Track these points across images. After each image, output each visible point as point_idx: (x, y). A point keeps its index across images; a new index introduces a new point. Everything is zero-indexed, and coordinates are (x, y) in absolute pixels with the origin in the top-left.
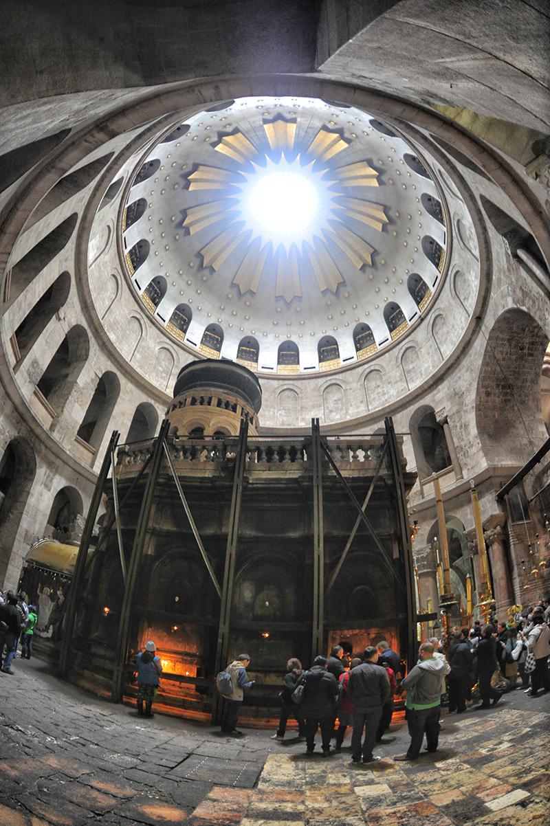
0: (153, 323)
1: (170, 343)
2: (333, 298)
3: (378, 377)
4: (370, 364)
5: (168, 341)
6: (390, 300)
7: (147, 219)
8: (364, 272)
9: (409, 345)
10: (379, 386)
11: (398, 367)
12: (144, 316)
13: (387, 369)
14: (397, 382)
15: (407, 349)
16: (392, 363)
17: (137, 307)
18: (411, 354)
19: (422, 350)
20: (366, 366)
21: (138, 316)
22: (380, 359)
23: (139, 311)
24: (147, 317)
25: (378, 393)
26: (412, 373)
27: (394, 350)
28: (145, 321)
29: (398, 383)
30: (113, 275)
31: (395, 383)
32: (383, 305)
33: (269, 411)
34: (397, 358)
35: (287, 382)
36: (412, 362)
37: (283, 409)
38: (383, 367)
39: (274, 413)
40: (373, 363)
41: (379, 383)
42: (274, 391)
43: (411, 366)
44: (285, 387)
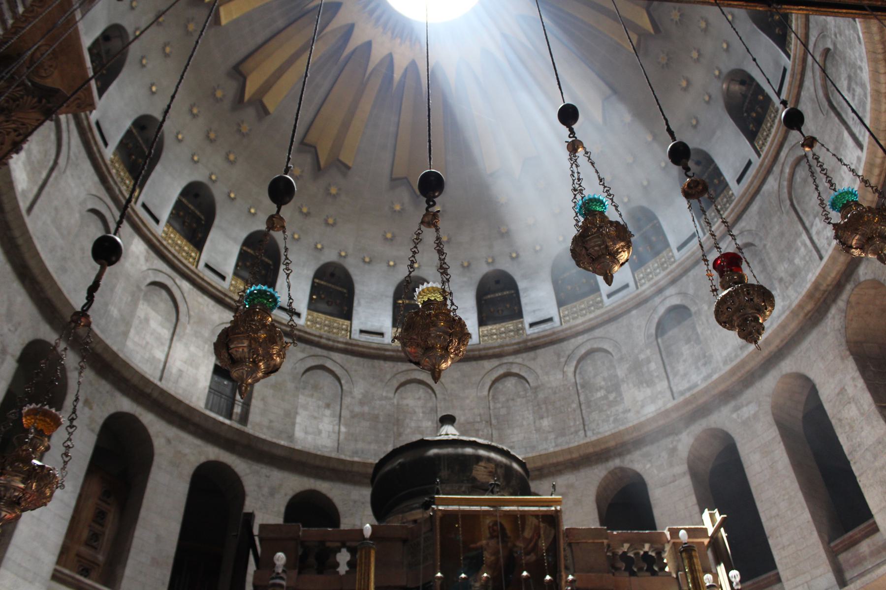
0: (535, 348)
1: (586, 337)
5: (580, 339)
7: (367, 267)
12: (510, 359)
17: (487, 364)
21: (501, 371)
23: (495, 362)
24: (516, 352)
28: (517, 363)
30: (403, 385)
33: (797, 250)
35: (783, 154)
37: (815, 217)
39: (805, 245)
42: (780, 201)
44: (787, 170)
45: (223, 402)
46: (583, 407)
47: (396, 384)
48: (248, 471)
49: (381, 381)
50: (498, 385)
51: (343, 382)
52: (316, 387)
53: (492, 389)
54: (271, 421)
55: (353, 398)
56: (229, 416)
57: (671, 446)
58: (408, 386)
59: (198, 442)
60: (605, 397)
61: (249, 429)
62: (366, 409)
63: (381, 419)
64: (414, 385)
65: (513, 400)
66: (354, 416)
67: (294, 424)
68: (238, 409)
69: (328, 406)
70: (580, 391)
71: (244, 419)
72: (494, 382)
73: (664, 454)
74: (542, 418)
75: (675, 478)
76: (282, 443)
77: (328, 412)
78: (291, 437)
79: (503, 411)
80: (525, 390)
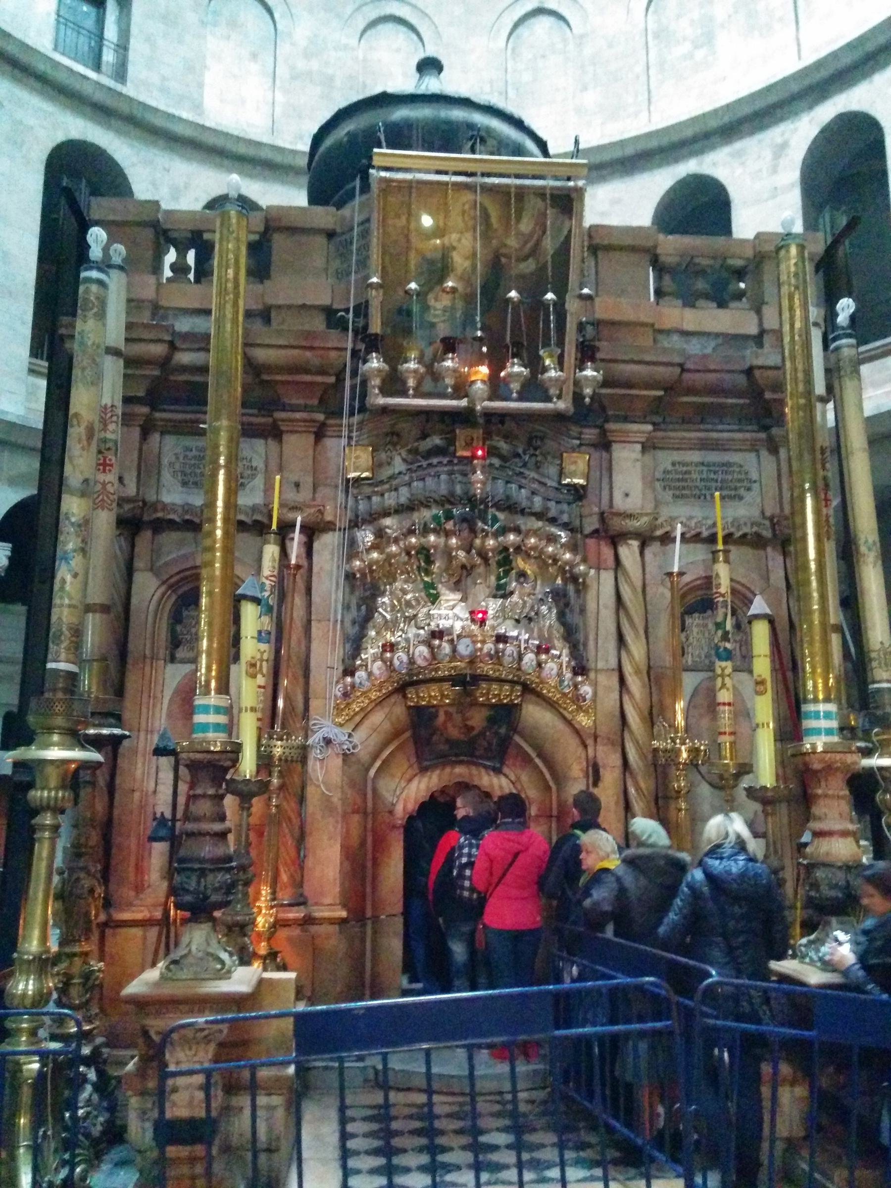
45: (84, 44)
46: (652, 72)
47: (361, 24)
48: (134, 159)
49: (338, 16)
50: (520, 30)
51: (277, 15)
52: (233, 24)
53: (514, 35)
54: (164, 79)
55: (293, 44)
56: (97, 66)
57: (779, 140)
58: (380, 27)
59: (47, 107)
60: (690, 56)
61: (129, 90)
62: (315, 65)
63: (338, 83)
64: (388, 28)
65: (543, 56)
66: (294, 77)
67: (201, 85)
68: (109, 57)
69: (254, 56)
70: (651, 44)
71: (121, 73)
72: (516, 26)
73: (768, 154)
74: (585, 89)
75: (775, 192)
76: (185, 115)
77: (254, 67)
78: (198, 107)
79: (526, 77)
80: (565, 40)
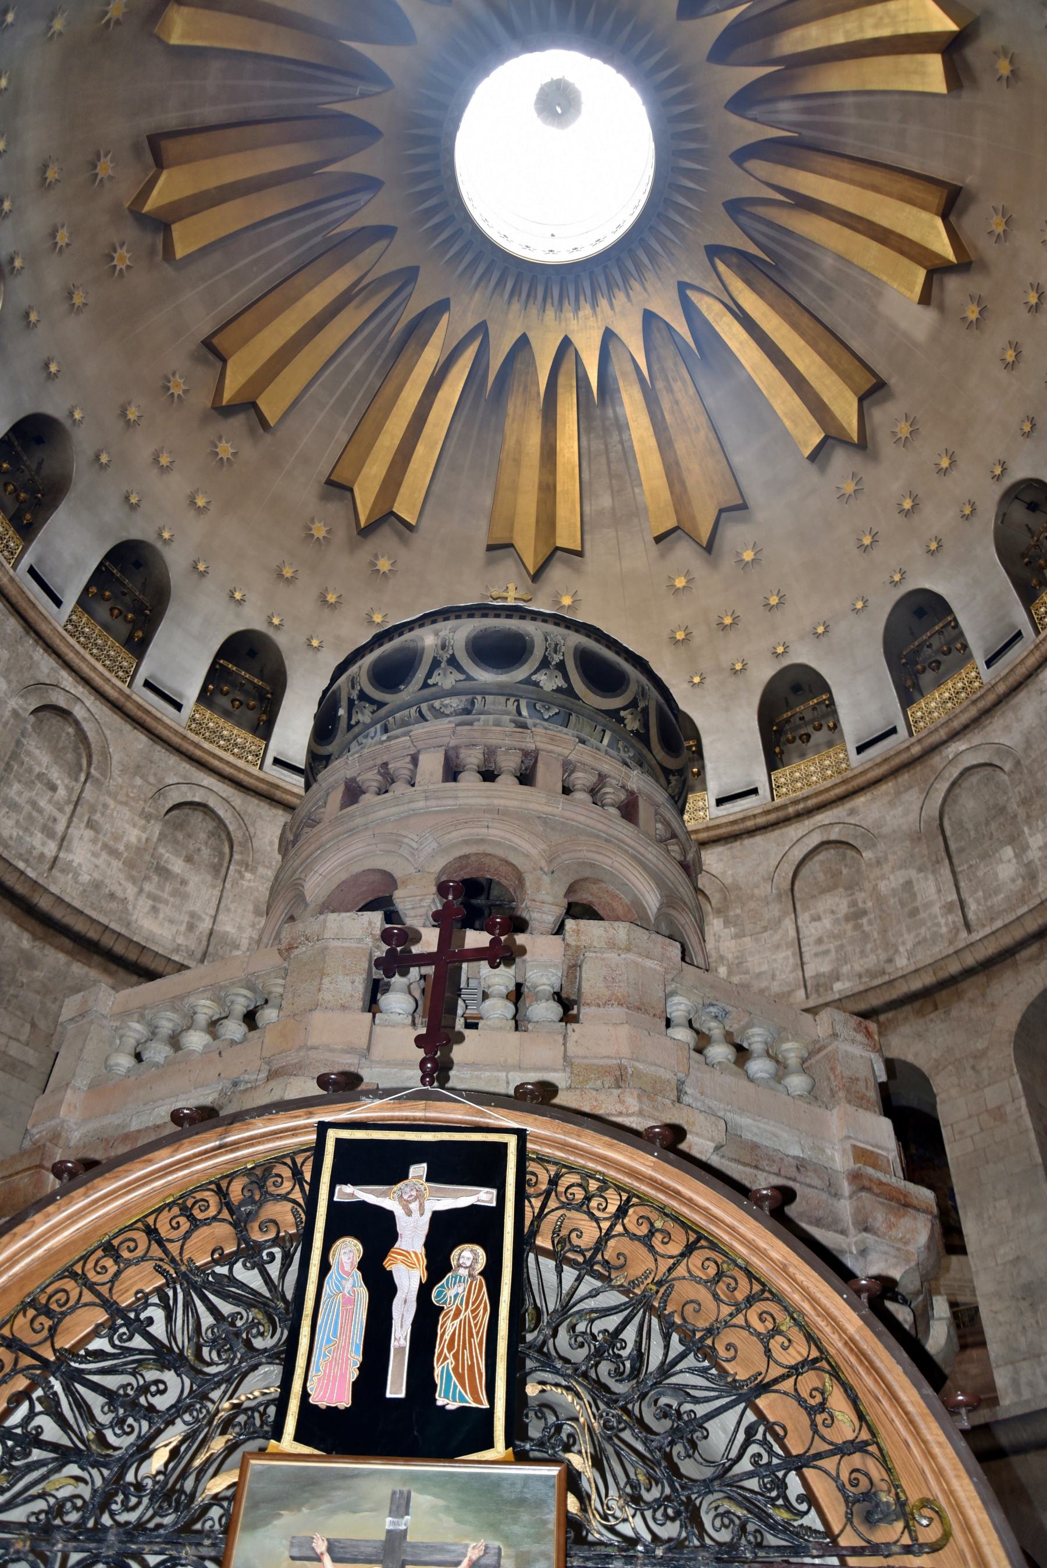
2: (202, 400)
3: (70, 756)
4: (80, 690)
6: (281, 640)
8: (325, 497)
9: (221, 813)
10: (53, 788)
11: (148, 817)
13: (117, 779)
14: (114, 853)
15: (202, 807)
16: (138, 781)
18: (203, 836)
19: (248, 875)
20: (66, 679)
22: (116, 720)
25: (34, 804)
26: (168, 888)
27: (173, 760)
29: (116, 864)
31: (105, 846)
32: (252, 619)
34: (161, 791)
36: (189, 859)
38: (105, 754)
40: (90, 701)
41: (55, 775)
43: (177, 866)
